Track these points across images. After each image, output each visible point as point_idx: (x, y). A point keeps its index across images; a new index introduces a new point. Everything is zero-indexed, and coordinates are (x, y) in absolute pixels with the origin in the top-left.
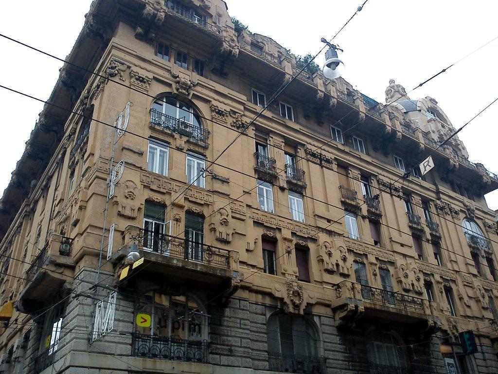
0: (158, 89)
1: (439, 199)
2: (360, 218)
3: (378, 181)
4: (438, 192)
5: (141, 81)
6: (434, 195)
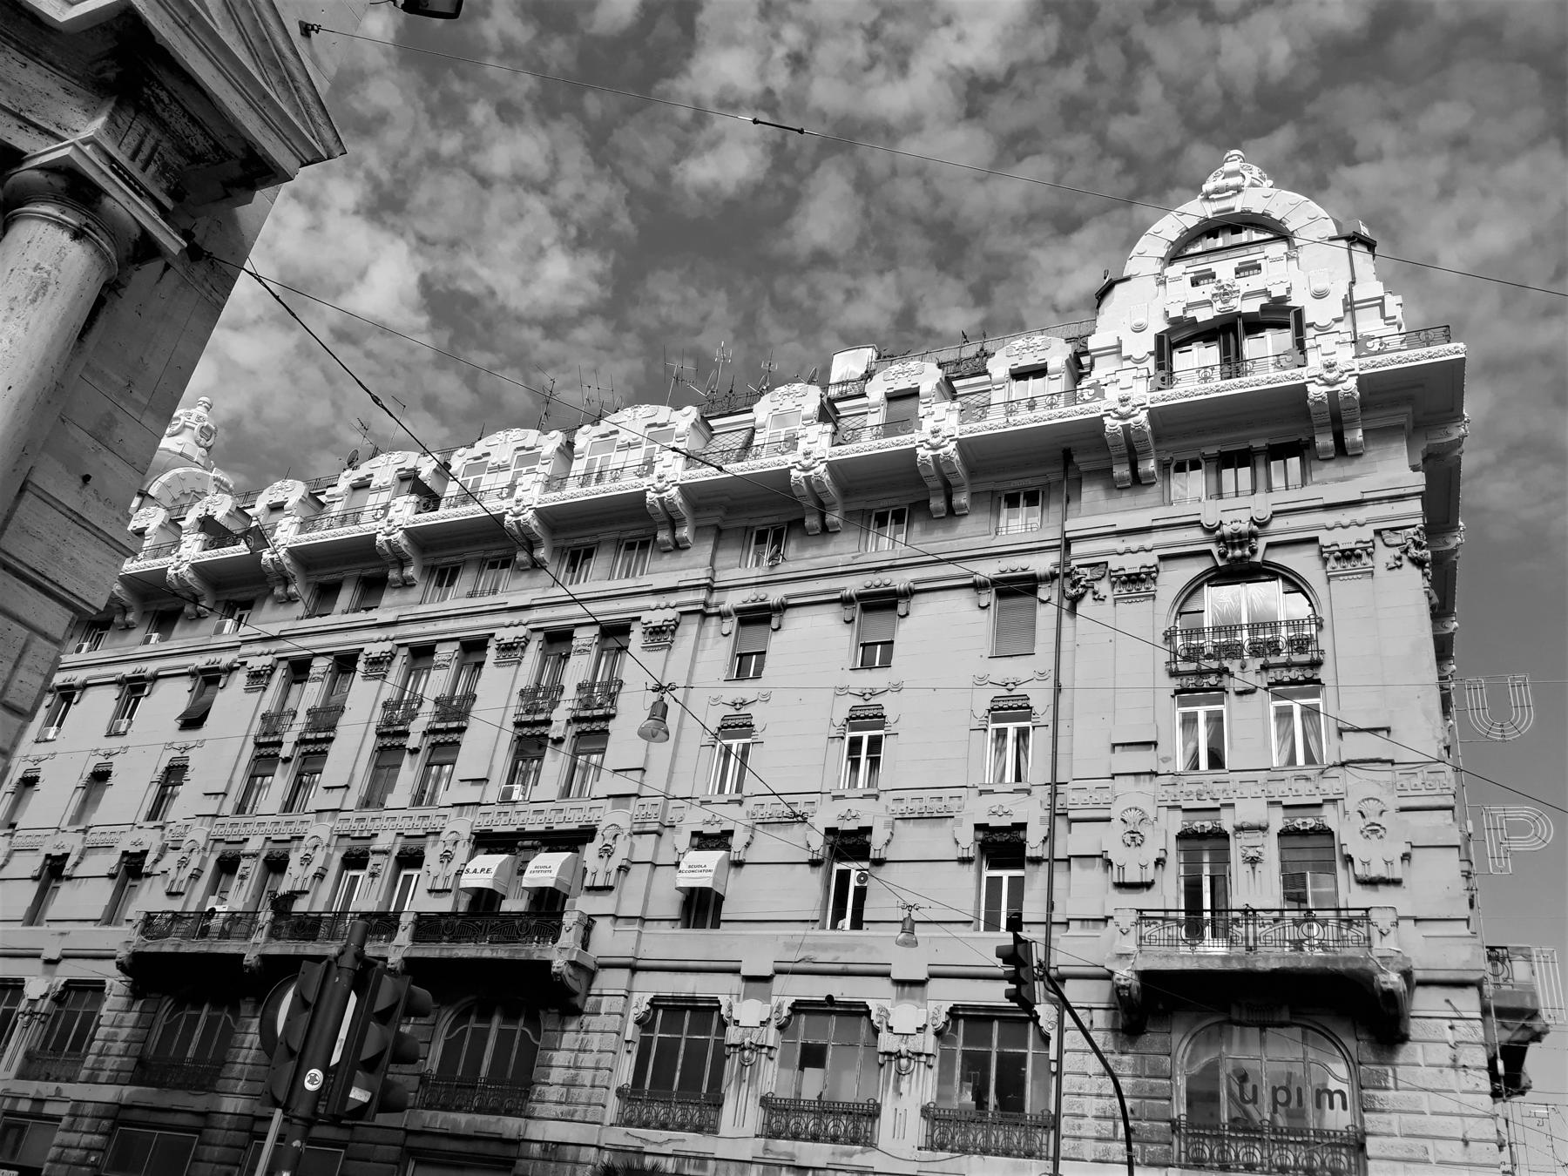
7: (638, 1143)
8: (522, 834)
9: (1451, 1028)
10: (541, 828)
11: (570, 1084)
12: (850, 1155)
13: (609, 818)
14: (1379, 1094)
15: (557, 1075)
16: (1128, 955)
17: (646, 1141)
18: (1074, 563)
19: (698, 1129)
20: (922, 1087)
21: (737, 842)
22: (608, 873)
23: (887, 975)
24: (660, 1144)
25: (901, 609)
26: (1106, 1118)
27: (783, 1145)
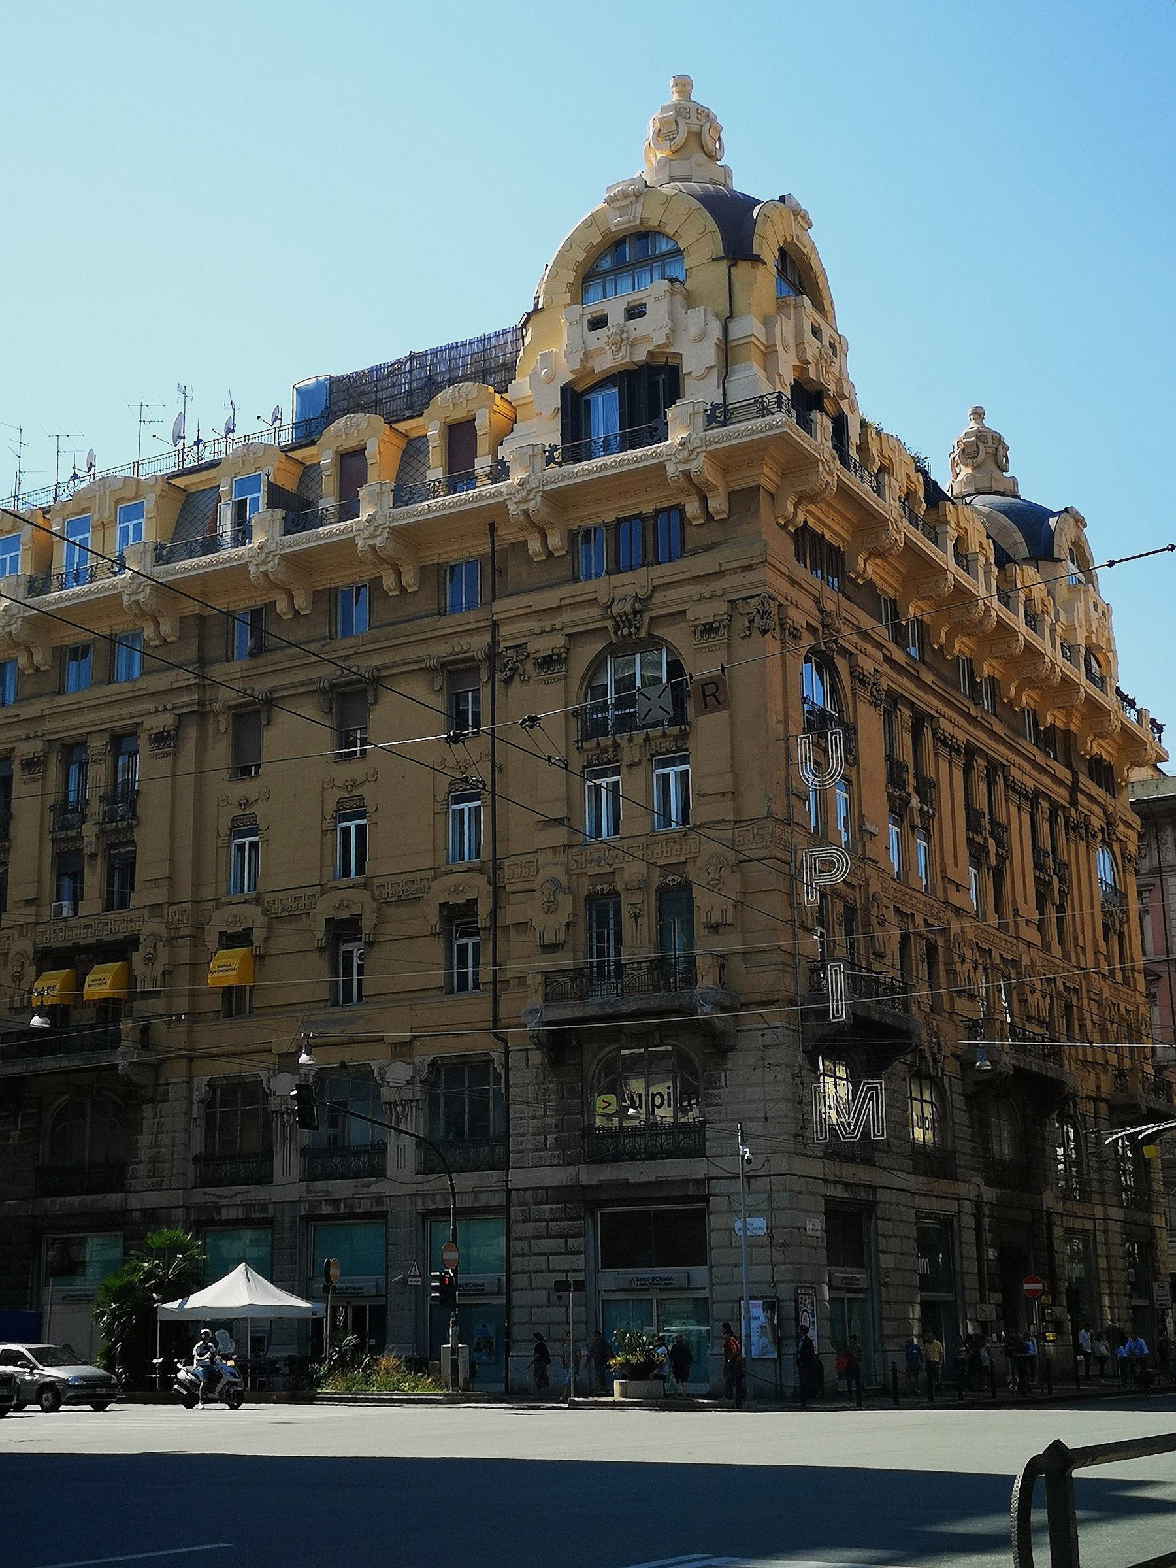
0: (807, 641)
1: (1074, 803)
2: (984, 869)
3: (1006, 780)
4: (1074, 789)
5: (795, 636)
6: (1065, 793)
7: (214, 1199)
8: (78, 949)
9: (763, 1035)
10: (93, 941)
11: (154, 1160)
12: (368, 1185)
13: (150, 927)
14: (715, 1092)
15: (145, 1154)
16: (536, 1011)
17: (220, 1197)
18: (503, 645)
19: (260, 1181)
20: (415, 1123)
21: (258, 936)
22: (154, 979)
23: (381, 1040)
24: (231, 1198)
25: (370, 699)
26: (539, 1134)
27: (320, 1185)
